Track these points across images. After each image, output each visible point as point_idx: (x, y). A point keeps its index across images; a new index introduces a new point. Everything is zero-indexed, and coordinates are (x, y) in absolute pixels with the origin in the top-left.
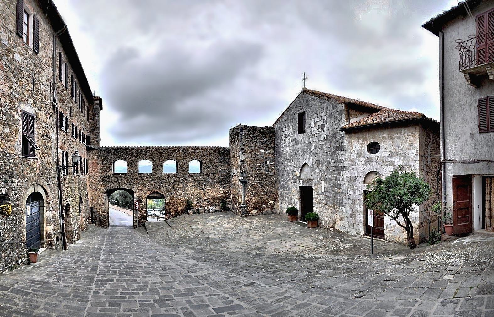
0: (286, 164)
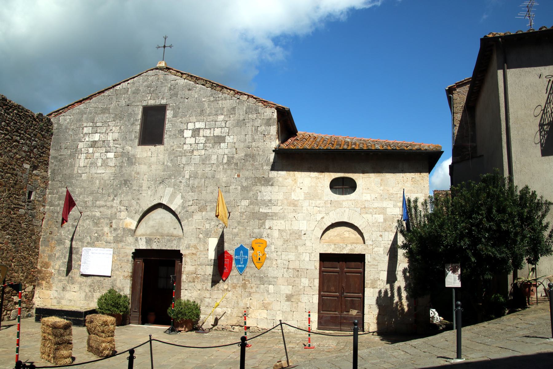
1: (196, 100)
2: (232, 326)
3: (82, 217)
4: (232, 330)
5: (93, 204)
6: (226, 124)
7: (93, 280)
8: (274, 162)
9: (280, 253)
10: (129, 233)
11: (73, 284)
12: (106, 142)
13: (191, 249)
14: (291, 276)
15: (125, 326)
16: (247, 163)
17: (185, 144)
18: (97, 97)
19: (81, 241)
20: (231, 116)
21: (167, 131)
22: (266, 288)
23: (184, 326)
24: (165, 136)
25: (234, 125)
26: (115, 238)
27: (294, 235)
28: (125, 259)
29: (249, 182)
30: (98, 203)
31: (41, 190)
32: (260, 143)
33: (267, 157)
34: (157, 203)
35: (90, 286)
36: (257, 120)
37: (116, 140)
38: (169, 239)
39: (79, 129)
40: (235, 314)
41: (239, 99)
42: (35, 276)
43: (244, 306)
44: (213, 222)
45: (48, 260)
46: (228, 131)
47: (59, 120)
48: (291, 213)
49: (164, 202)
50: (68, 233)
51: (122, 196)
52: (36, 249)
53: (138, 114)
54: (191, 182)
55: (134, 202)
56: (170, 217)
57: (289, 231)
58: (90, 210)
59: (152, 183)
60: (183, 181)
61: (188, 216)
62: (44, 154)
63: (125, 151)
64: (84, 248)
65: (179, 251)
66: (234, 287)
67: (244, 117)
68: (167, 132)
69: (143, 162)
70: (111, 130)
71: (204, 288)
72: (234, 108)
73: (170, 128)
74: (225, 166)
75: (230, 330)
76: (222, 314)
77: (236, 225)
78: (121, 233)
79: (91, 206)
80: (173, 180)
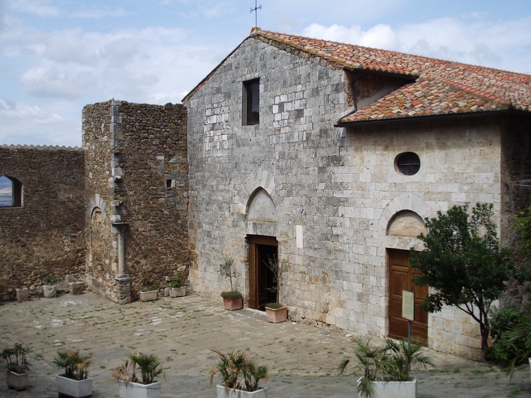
0: (215, 188)
13: (283, 236)
14: (361, 272)
17: (274, 121)
29: (324, 163)
71: (295, 278)
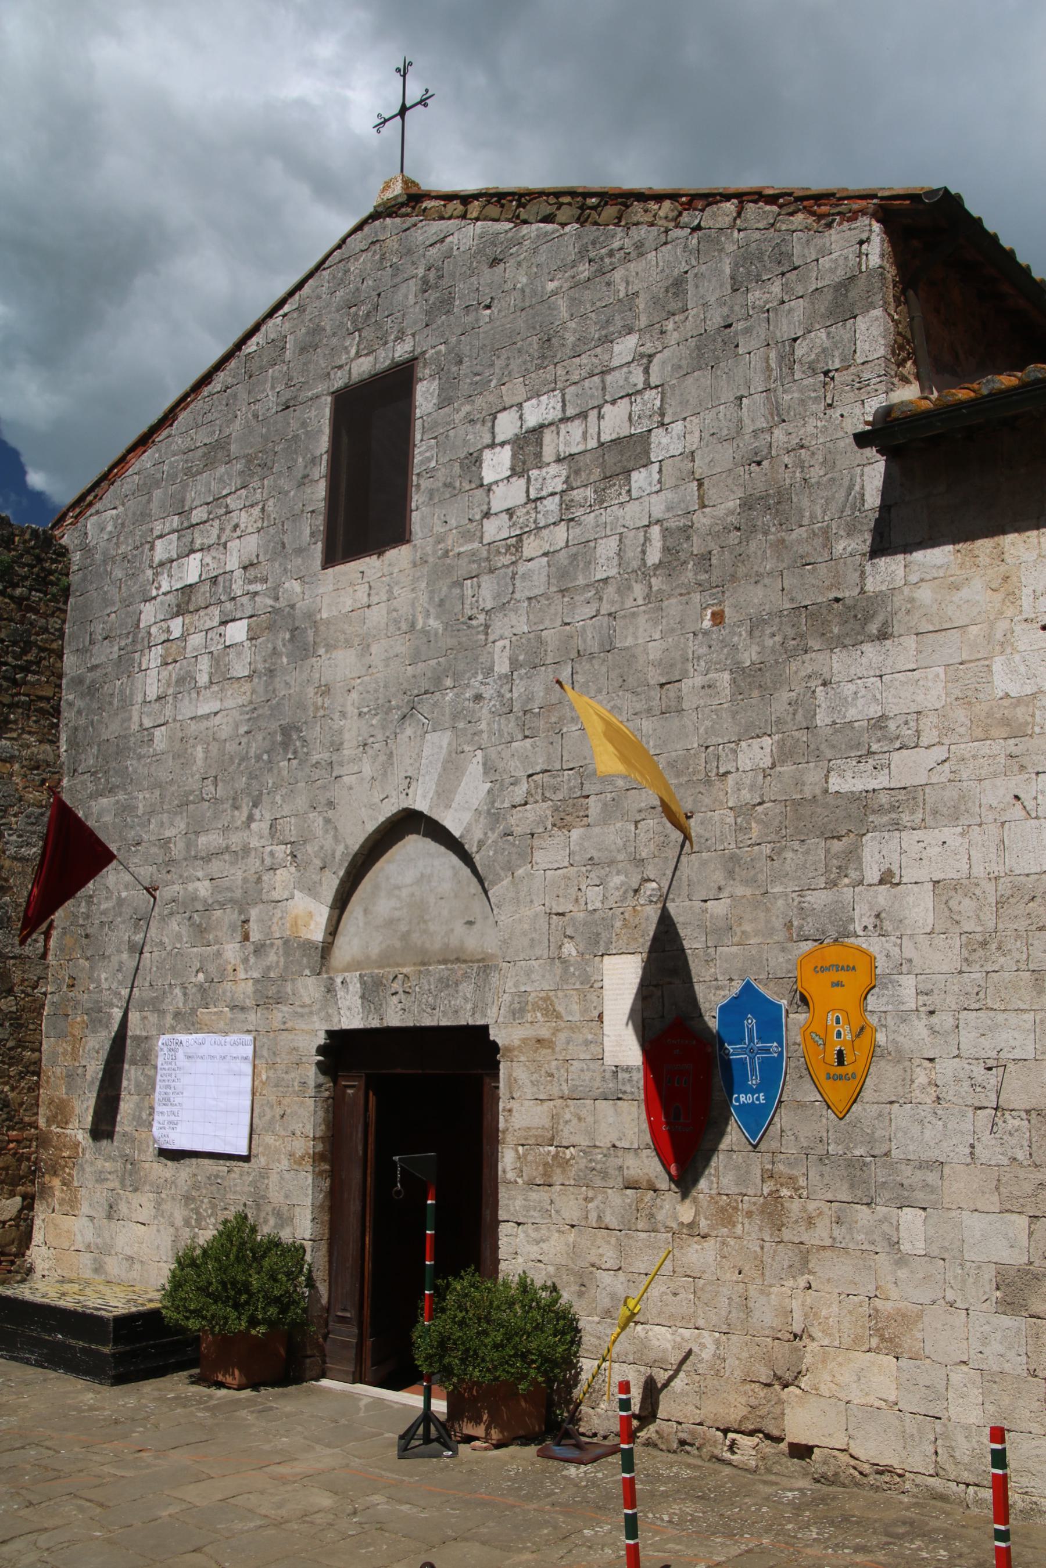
0: (178, 850)
1: (524, 301)
2: (725, 1431)
3: (156, 909)
4: (727, 1455)
5: (188, 846)
6: (647, 371)
7: (195, 1175)
8: (885, 508)
9: (950, 1022)
10: (305, 960)
11: (136, 1190)
12: (221, 579)
13: (529, 1017)
14: (1020, 1155)
15: (292, 1389)
16: (753, 546)
17: (487, 515)
18: (192, 406)
19: (155, 1005)
20: (670, 326)
21: (418, 474)
22: (885, 1227)
23: (485, 1417)
24: (417, 499)
25: (684, 363)
26: (259, 987)
27: (1021, 909)
28: (293, 1080)
29: (769, 643)
30: (202, 840)
31: (28, 817)
32: (812, 421)
33: (851, 488)
34: (394, 810)
35: (188, 1199)
36: (786, 306)
37: (252, 565)
38: (446, 973)
39: (143, 552)
40: (734, 1367)
41: (698, 228)
42: (28, 1159)
43: (777, 1323)
44: (618, 873)
45: (67, 1094)
46: (658, 403)
47: (86, 534)
48: (995, 776)
49: (421, 806)
50: (120, 976)
51: (278, 798)
52: (24, 1048)
53: (320, 431)
54: (519, 690)
55: (317, 821)
56: (449, 873)
57: (990, 887)
58: (181, 876)
59: (374, 722)
60: (488, 692)
61: (514, 857)
62: (34, 673)
63: (281, 604)
64: (163, 1039)
65: (485, 1029)
66: (726, 1215)
67: (725, 310)
68: (421, 482)
69: (342, 637)
70: (236, 526)
71: (593, 1216)
72: (678, 285)
73: (429, 460)
74: (653, 580)
75: (717, 1452)
76: (675, 1358)
77: (718, 877)
78: (278, 962)
79: (181, 857)
80: (451, 695)
